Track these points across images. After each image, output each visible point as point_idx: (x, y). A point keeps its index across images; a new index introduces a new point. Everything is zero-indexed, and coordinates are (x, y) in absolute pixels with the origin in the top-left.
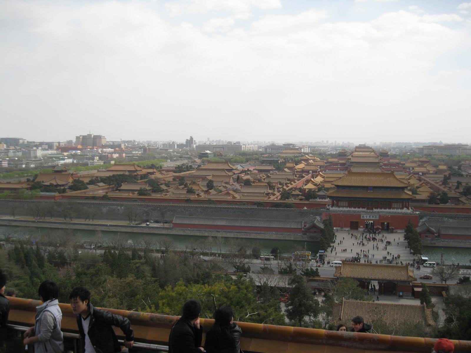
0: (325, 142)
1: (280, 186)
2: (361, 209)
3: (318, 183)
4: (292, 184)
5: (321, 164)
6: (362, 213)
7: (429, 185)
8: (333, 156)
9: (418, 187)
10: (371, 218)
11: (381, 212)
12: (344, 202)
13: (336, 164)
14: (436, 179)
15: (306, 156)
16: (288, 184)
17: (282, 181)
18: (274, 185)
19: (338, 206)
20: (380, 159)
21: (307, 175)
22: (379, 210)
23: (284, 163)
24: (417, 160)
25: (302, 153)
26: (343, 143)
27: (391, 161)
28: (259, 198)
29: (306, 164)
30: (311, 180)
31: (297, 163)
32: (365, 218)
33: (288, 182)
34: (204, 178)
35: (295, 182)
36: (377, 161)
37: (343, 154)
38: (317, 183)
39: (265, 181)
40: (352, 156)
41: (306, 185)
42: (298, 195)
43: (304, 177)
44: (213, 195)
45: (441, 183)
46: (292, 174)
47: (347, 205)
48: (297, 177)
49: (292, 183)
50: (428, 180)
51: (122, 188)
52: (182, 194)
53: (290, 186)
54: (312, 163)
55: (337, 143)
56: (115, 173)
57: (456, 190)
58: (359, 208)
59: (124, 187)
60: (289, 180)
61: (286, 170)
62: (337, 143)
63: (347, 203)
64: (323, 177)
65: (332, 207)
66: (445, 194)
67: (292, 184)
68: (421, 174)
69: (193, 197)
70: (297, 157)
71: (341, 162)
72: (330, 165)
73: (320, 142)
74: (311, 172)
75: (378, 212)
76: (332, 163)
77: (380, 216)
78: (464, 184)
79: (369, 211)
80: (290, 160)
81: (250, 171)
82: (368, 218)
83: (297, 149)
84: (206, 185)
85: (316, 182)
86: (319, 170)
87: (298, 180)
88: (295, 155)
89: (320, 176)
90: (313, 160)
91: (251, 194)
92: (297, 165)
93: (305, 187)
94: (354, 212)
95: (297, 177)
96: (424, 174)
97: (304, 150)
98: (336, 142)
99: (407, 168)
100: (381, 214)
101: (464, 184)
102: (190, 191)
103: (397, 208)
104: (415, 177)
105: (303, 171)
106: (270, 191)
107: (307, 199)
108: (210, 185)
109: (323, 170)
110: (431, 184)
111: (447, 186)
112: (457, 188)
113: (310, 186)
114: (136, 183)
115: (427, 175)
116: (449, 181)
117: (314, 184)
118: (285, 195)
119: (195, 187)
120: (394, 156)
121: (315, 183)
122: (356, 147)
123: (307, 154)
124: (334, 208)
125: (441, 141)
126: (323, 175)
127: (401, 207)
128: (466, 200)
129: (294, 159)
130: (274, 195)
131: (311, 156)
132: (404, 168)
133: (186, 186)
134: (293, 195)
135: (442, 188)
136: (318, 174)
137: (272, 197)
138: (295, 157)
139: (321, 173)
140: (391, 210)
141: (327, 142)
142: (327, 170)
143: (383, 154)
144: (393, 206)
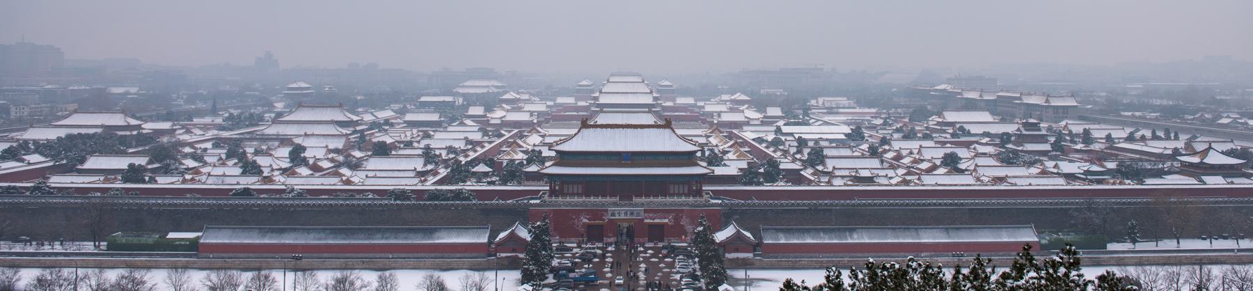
1: (452, 156)
2: (608, 199)
3: (530, 148)
9: (725, 152)
17: (457, 145)
18: (437, 152)
19: (564, 195)
20: (655, 99)
22: (643, 200)
23: (465, 107)
28: (404, 182)
31: (489, 109)
34: (284, 141)
35: (483, 147)
39: (422, 146)
42: (486, 174)
44: (304, 180)
46: (476, 129)
51: (87, 166)
52: (230, 176)
53: (472, 155)
56: (75, 131)
57: (798, 156)
58: (604, 196)
59: (93, 163)
60: (468, 142)
61: (468, 122)
65: (550, 196)
66: (773, 164)
69: (251, 182)
78: (811, 144)
81: (392, 125)
87: (490, 143)
91: (390, 174)
96: (738, 125)
101: (811, 144)
102: (251, 168)
103: (679, 195)
106: (430, 167)
107: (504, 183)
108: (297, 155)
110: (751, 146)
112: (799, 151)
114: (123, 153)
118: (459, 172)
119: (262, 161)
128: (813, 174)
130: (436, 173)
133: (242, 157)
134: (475, 173)
135: (770, 151)
137: (432, 180)
140: (669, 199)
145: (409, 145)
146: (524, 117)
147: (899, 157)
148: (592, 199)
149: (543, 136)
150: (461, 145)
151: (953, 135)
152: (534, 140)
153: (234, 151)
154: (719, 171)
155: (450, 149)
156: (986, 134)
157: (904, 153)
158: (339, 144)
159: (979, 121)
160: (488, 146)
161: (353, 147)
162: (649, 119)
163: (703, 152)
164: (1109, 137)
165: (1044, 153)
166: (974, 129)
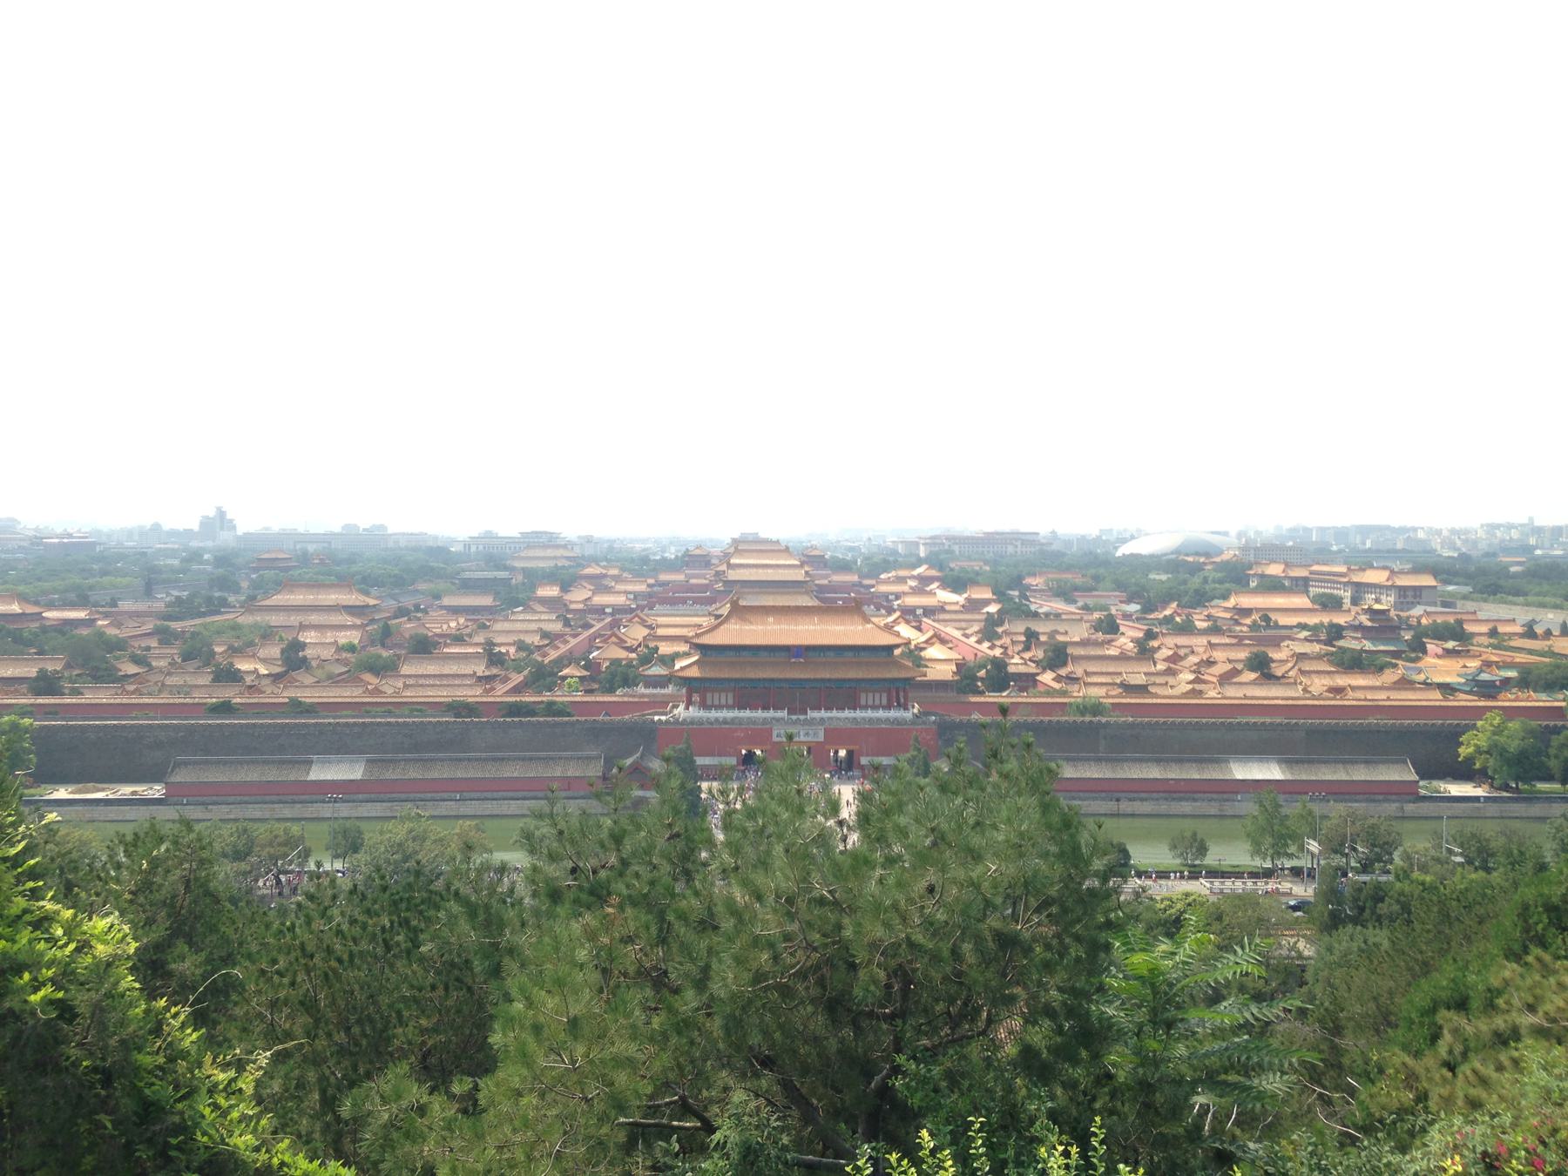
14: (964, 625)
17: (528, 639)
60: (545, 635)
84: (278, 656)
87: (575, 636)
104: (908, 622)
111: (998, 643)
115: (942, 616)
116: (1000, 630)
145: (459, 639)
147: (1175, 658)
149: (650, 627)
150: (536, 640)
151: (1254, 626)
153: (196, 652)
155: (521, 646)
156: (1303, 627)
157: (1182, 652)
158: (354, 637)
159: (1289, 607)
160: (573, 642)
161: (373, 643)
164: (1493, 633)
165: (1396, 655)
166: (1284, 620)
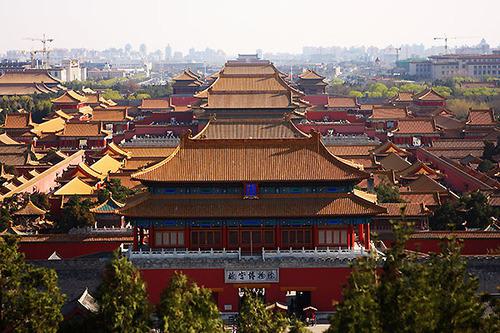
0: (136, 48)
2: (224, 253)
4: (18, 184)
5: (119, 117)
6: (227, 265)
7: (438, 172)
8: (155, 92)
10: (256, 279)
11: (287, 258)
12: (173, 235)
13: (163, 117)
15: (71, 93)
16: (9, 182)
19: (153, 246)
21: (71, 154)
22: (279, 253)
24: (409, 98)
25: (59, 83)
26: (191, 50)
27: (332, 104)
29: (69, 117)
30: (78, 168)
31: (40, 116)
32: (238, 279)
33: (9, 177)
35: (30, 177)
36: (282, 103)
37: (184, 88)
38: (99, 177)
40: (211, 92)
41: (63, 184)
42: (33, 217)
43: (63, 159)
45: (475, 166)
47: (181, 242)
48: (36, 160)
49: (21, 179)
50: (437, 155)
54: (90, 116)
55: (172, 54)
58: (218, 248)
62: (172, 54)
63: (181, 236)
64: (118, 160)
65: (136, 249)
67: (18, 184)
68: (417, 142)
70: (45, 97)
71: (178, 109)
72: (146, 122)
73: (121, 50)
74: (83, 143)
75: (277, 260)
76: (148, 112)
77: (282, 271)
79: (247, 257)
80: (19, 108)
82: (247, 278)
83: (45, 73)
85: (95, 175)
86: (110, 137)
87: (40, 170)
88: (38, 92)
89: (110, 155)
90: (92, 106)
92: (39, 121)
93: (63, 191)
94: (204, 261)
95: (36, 160)
96: (425, 140)
97: (68, 73)
98: (168, 49)
99: (376, 125)
100: (284, 265)
103: (334, 246)
105: (53, 141)
109: (121, 137)
113: (76, 187)
115: (435, 145)
117: (90, 180)
120: (340, 92)
121: (93, 177)
122: (229, 64)
123: (76, 86)
124: (141, 254)
125: (483, 41)
126: (122, 152)
127: (344, 241)
129: (32, 105)
131: (87, 94)
132: (369, 125)
136: (105, 150)
138: (37, 97)
139: (112, 145)
140: (316, 253)
141: (143, 48)
142: (135, 137)
143: (311, 86)
144: (321, 241)
146: (92, 132)
148: (199, 254)
152: (106, 166)
154: (393, 209)
162: (282, 133)
163: (371, 181)
